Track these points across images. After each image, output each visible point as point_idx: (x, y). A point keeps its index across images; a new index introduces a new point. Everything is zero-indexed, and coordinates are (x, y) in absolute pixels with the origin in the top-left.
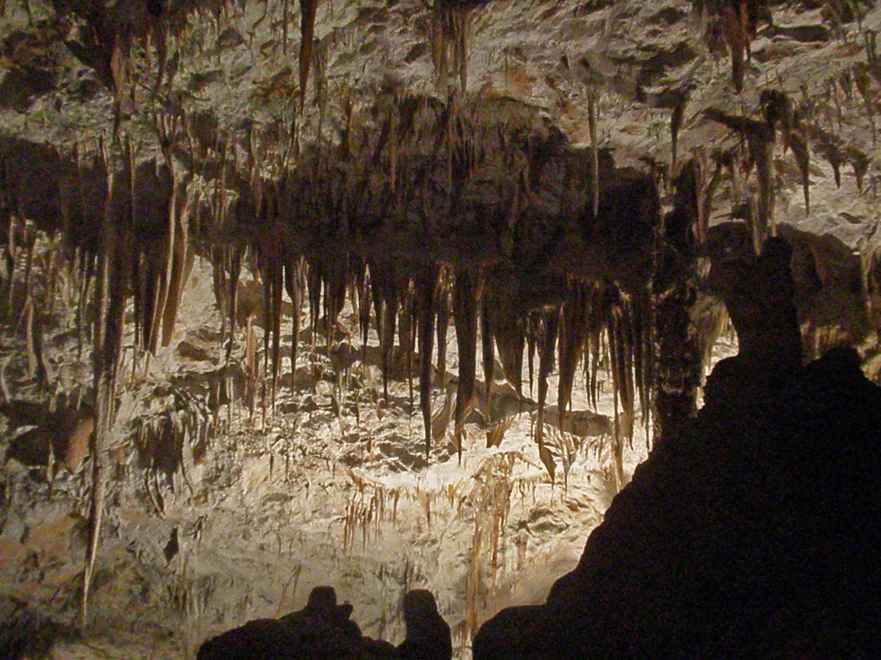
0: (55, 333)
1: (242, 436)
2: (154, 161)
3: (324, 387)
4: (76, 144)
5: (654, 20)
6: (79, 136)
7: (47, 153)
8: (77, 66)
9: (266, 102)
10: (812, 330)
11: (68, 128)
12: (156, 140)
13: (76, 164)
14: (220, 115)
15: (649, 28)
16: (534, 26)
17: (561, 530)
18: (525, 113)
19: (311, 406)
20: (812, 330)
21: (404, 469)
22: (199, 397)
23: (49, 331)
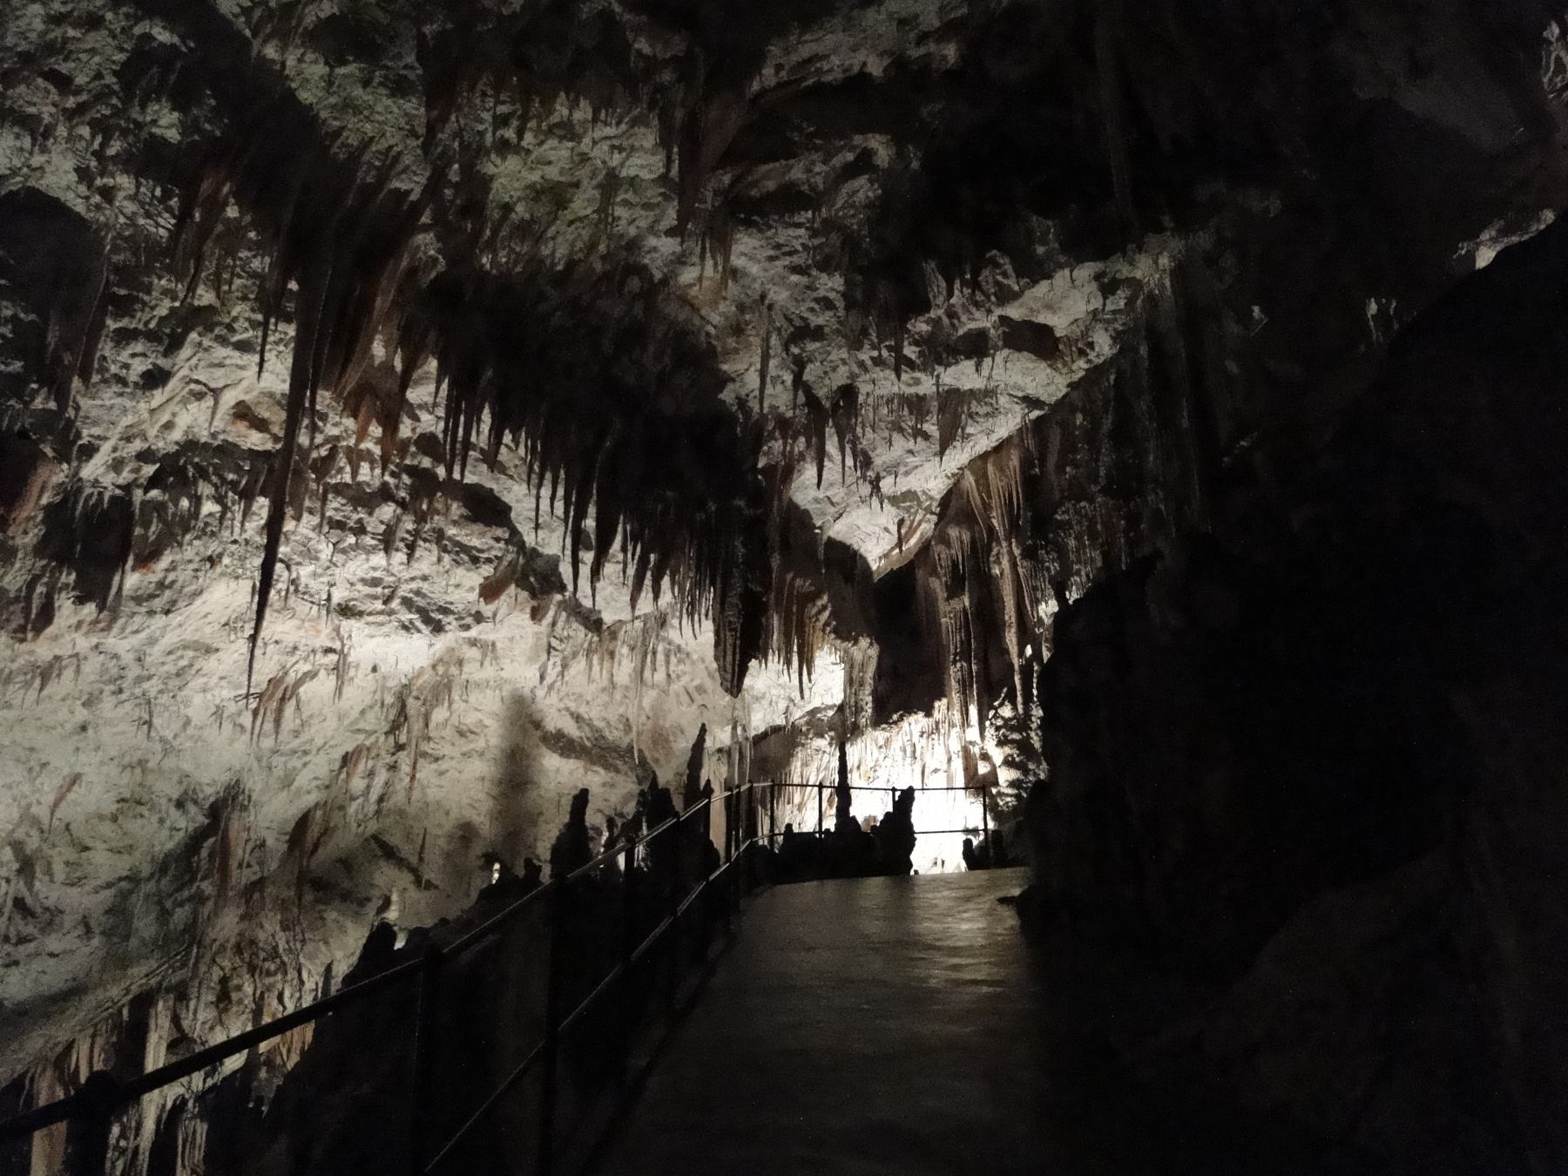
0: (124, 323)
1: (235, 546)
2: (408, 192)
3: (387, 511)
4: (343, 128)
5: (817, 300)
6: (352, 121)
7: (306, 118)
8: (411, 59)
9: (536, 199)
10: (794, 579)
11: (348, 106)
12: (427, 174)
13: (329, 147)
14: (495, 185)
15: (813, 304)
16: (759, 262)
17: (437, 760)
18: (697, 321)
19: (360, 530)
20: (794, 579)
21: (419, 631)
22: (231, 476)
23: (117, 316)
